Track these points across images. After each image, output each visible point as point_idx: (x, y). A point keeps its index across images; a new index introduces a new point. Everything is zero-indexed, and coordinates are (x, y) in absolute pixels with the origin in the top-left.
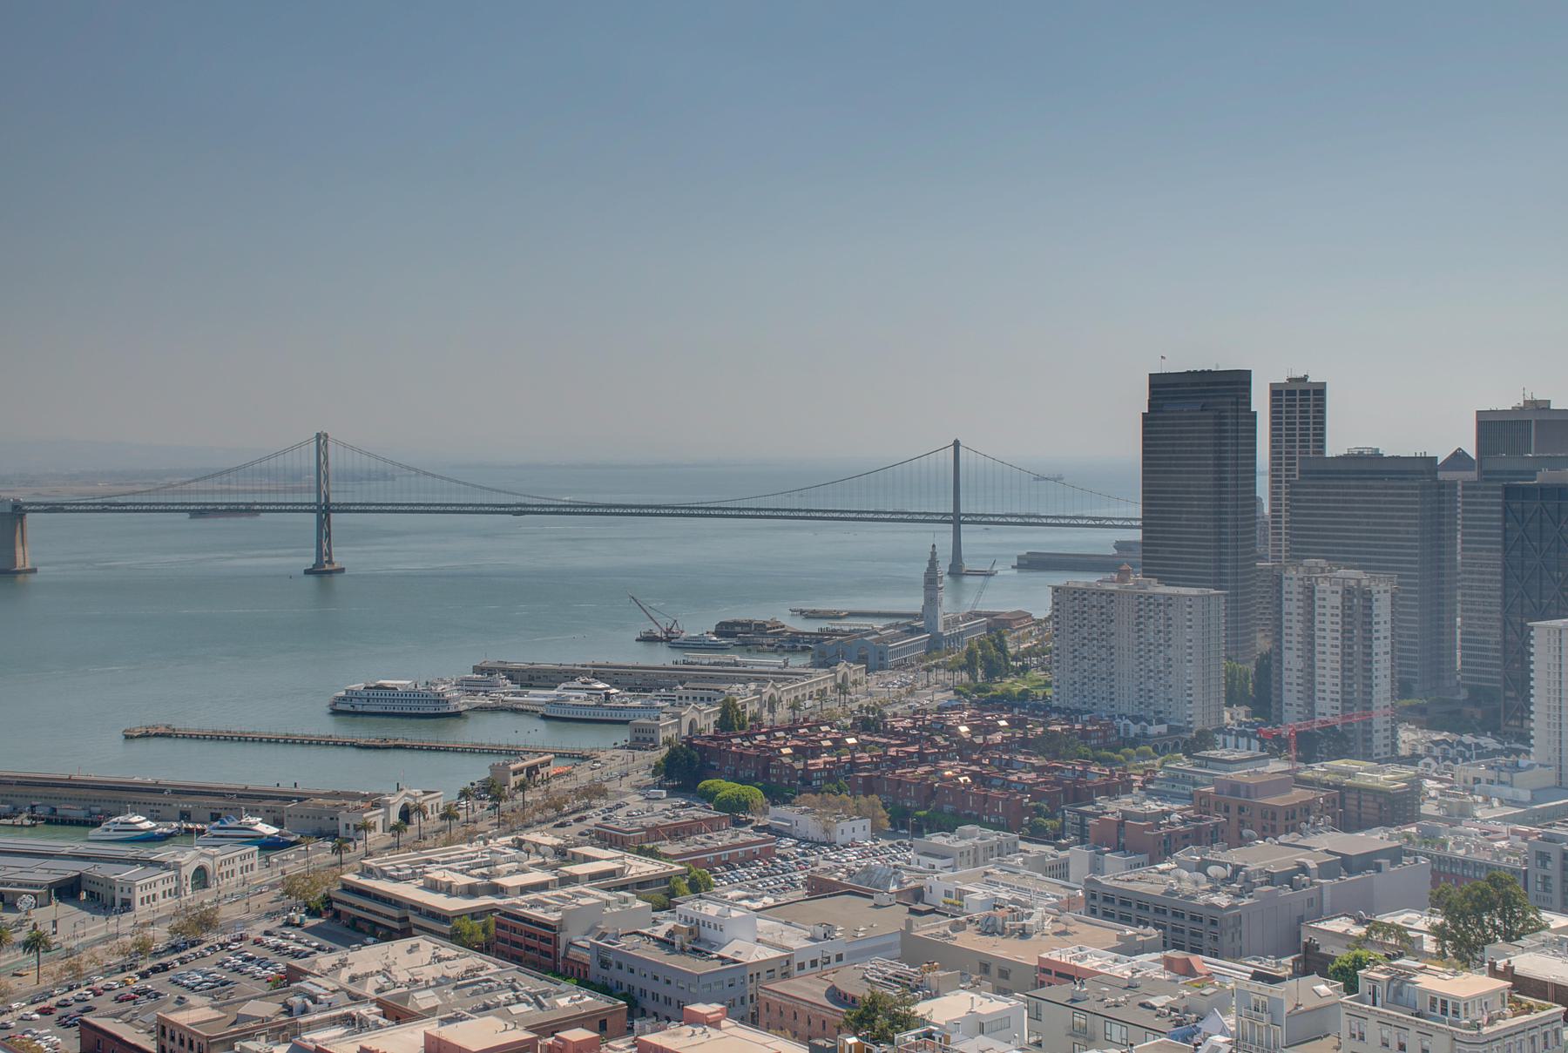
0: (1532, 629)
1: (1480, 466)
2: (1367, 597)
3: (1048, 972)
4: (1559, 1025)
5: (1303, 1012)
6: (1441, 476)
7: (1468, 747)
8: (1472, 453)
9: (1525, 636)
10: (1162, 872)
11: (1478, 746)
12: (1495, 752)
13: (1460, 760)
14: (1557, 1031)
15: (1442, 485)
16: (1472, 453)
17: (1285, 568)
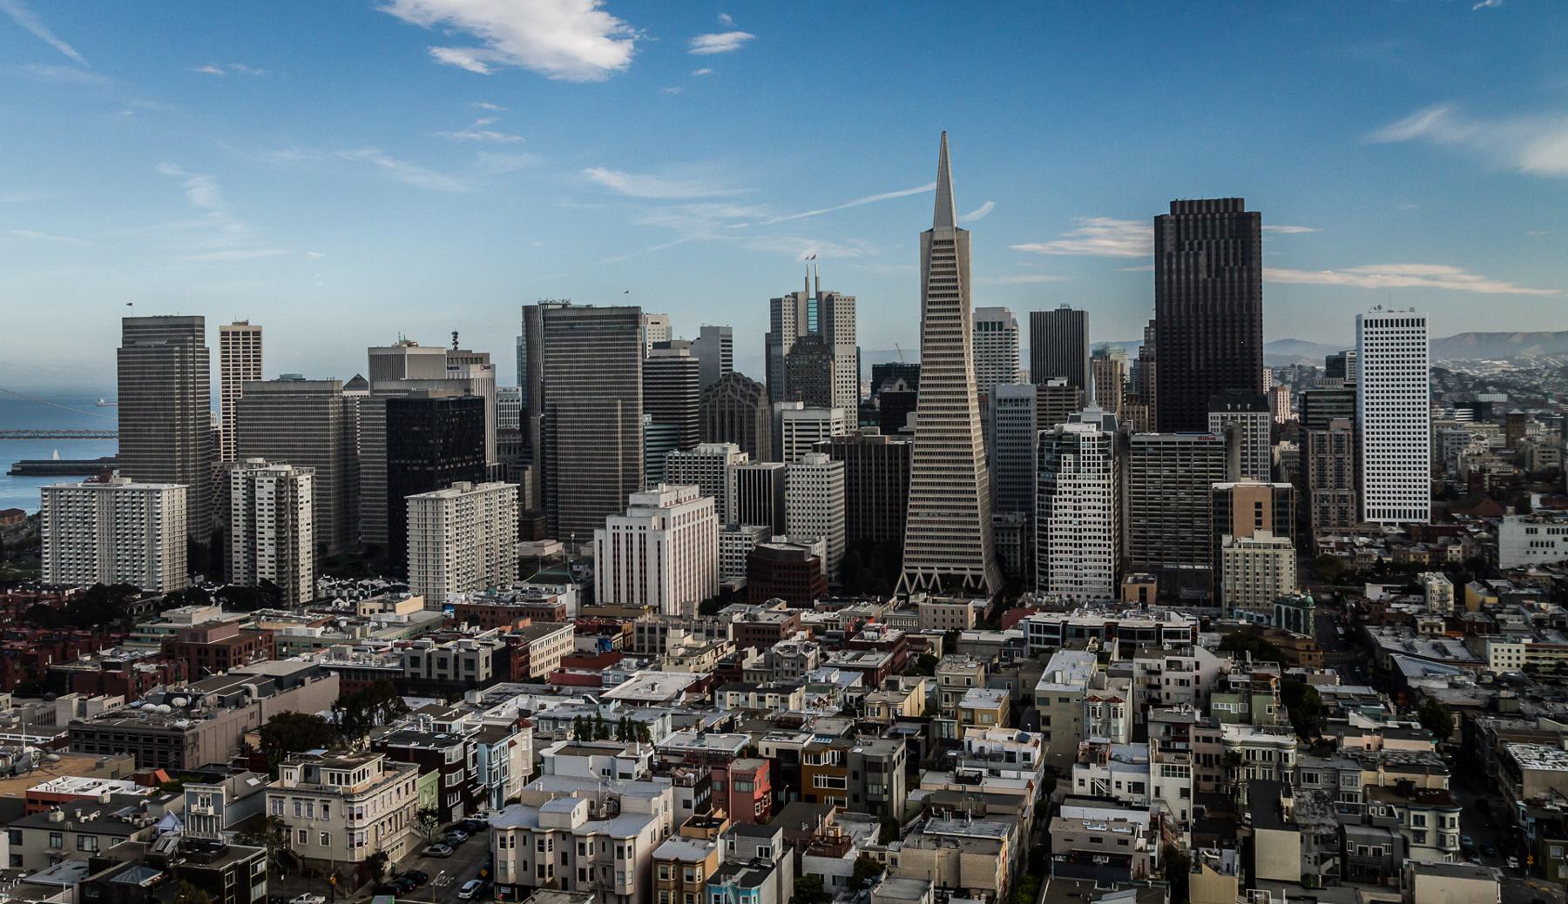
0: (407, 500)
1: (372, 387)
2: (294, 483)
3: (36, 802)
4: (416, 777)
5: (237, 801)
6: (346, 393)
7: (366, 588)
8: (366, 377)
9: (404, 503)
10: (133, 708)
11: (373, 586)
12: (385, 589)
13: (361, 598)
14: (414, 781)
15: (345, 400)
16: (366, 377)
17: (233, 466)
